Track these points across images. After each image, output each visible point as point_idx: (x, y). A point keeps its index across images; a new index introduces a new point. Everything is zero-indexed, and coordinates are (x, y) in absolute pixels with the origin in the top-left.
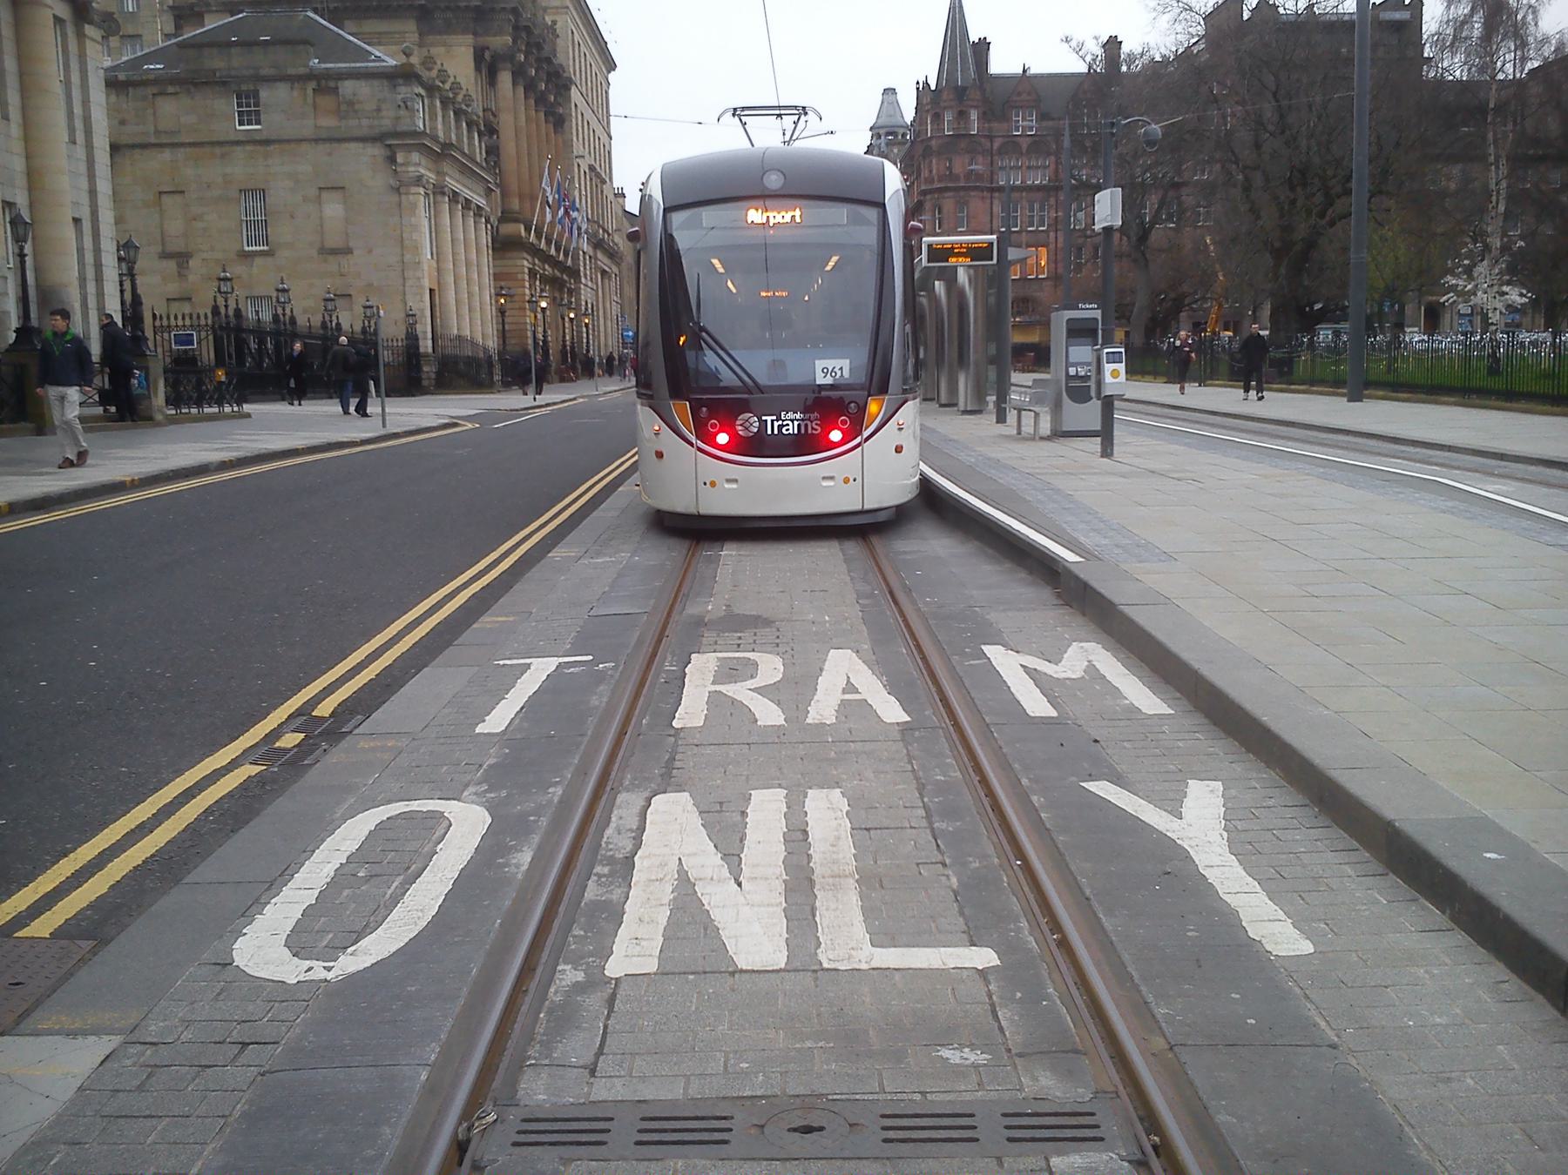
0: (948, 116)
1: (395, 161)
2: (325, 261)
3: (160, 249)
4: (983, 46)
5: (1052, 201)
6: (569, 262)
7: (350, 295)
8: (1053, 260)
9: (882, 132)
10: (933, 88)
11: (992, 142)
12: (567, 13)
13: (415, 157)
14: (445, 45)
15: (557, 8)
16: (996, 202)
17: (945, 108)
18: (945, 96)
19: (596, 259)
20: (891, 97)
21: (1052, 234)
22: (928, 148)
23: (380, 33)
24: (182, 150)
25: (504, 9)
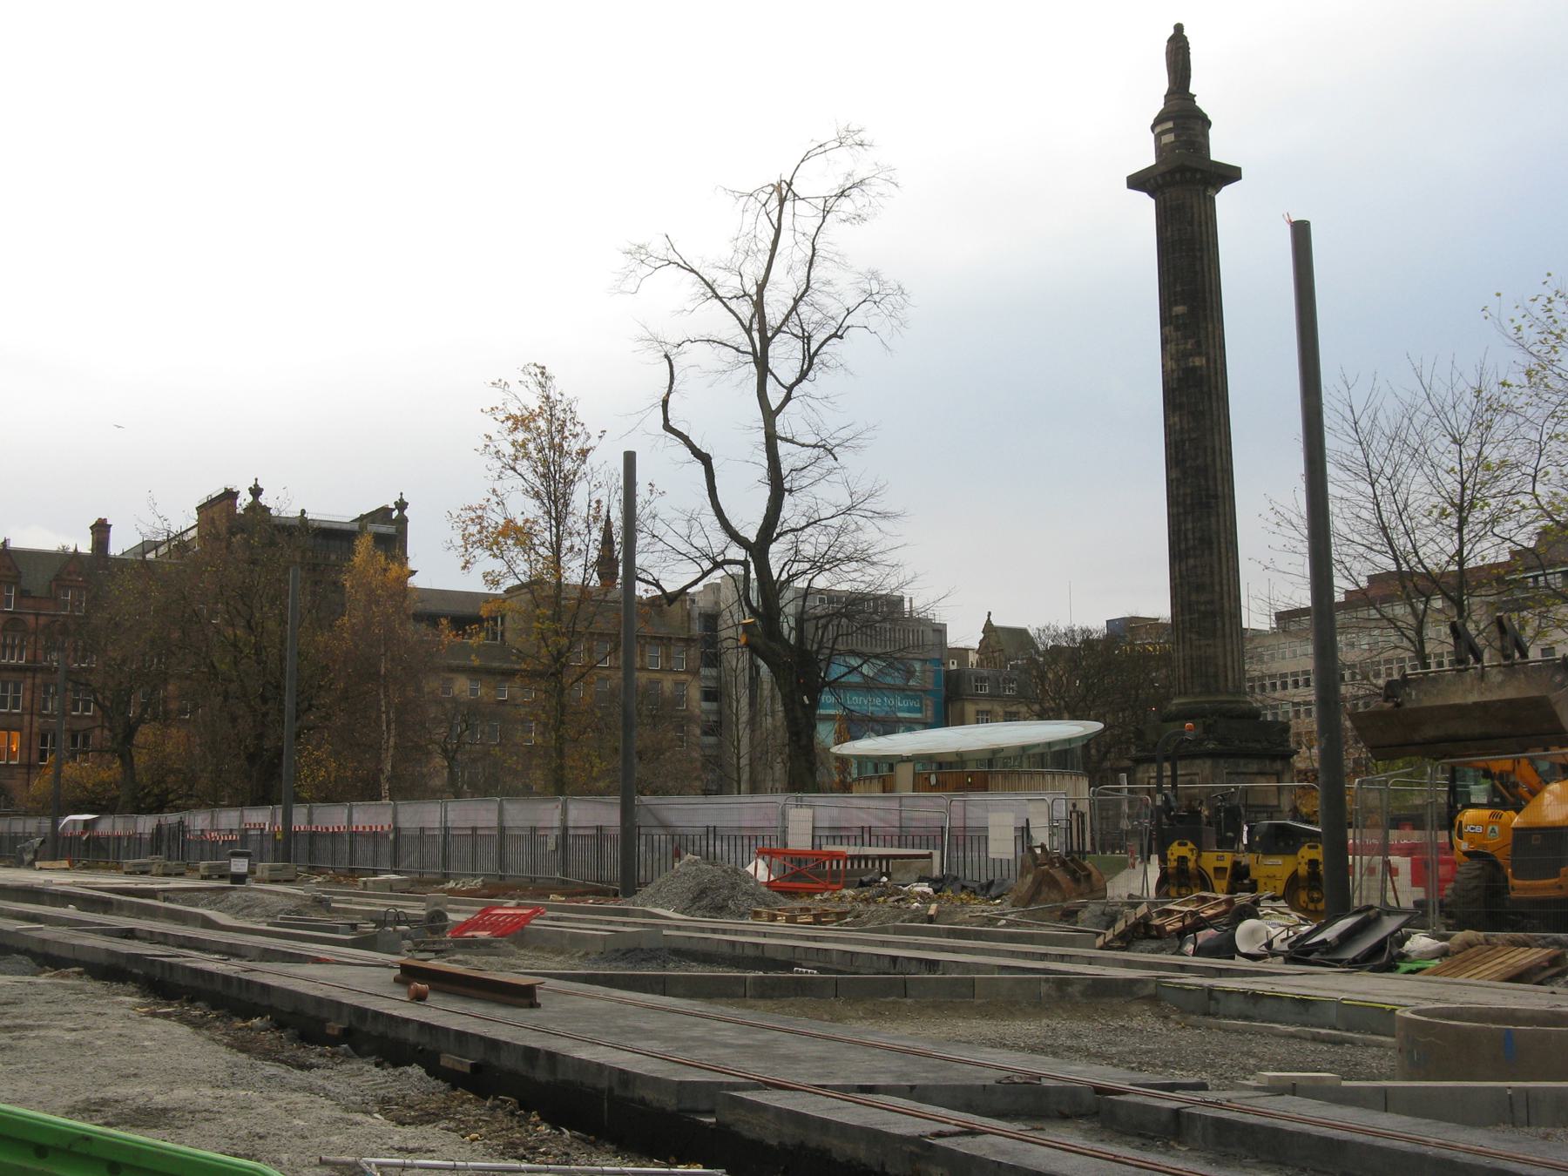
5: (29, 681)
8: (26, 746)
21: (27, 718)
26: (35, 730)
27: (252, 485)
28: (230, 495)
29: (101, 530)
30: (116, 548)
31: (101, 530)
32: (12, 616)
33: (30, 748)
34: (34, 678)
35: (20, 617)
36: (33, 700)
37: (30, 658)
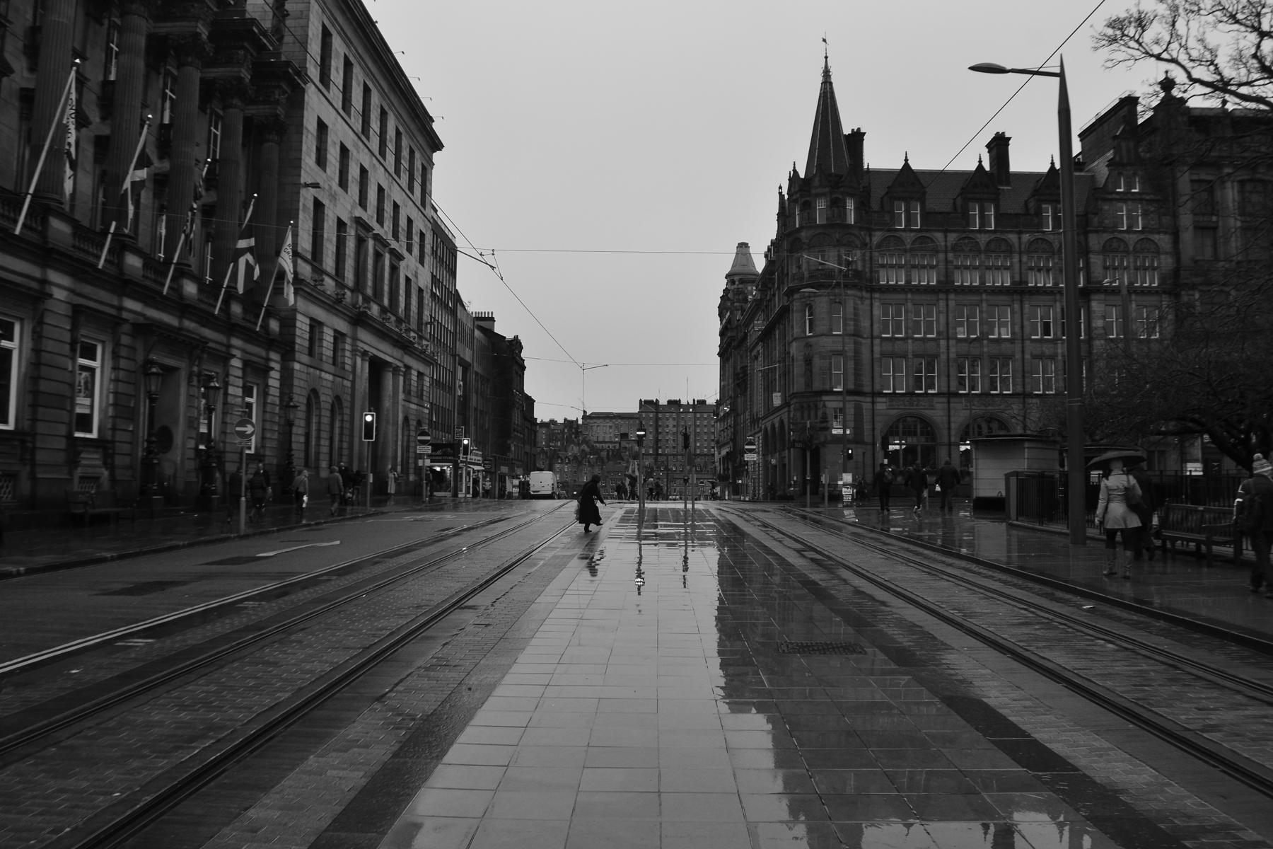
0: (821, 205)
4: (858, 137)
5: (942, 304)
6: (274, 325)
9: (736, 278)
10: (802, 175)
11: (870, 236)
16: (876, 304)
17: (818, 195)
18: (816, 182)
19: (355, 339)
20: (744, 250)
22: (799, 239)
26: (952, 356)
27: (1162, 77)
28: (1129, 103)
29: (999, 145)
30: (1017, 164)
31: (999, 145)
32: (920, 235)
33: (948, 376)
34: (947, 300)
35: (928, 235)
36: (947, 324)
37: (942, 279)
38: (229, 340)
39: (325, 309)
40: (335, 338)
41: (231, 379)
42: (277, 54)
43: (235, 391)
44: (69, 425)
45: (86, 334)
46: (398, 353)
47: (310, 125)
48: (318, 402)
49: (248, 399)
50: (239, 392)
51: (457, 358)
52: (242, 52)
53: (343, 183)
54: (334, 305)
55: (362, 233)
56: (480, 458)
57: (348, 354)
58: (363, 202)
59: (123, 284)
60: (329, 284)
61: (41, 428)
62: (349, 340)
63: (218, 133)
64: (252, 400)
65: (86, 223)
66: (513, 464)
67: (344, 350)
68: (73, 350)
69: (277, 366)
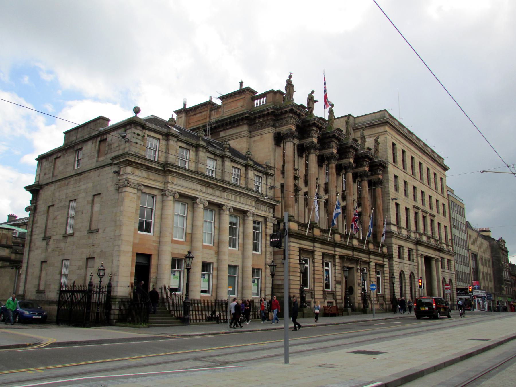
1: (120, 174)
2: (89, 238)
3: (43, 235)
6: (385, 250)
7: (94, 258)
12: (386, 134)
13: (129, 169)
14: (260, 134)
15: (382, 132)
19: (417, 250)
23: (232, 134)
24: (57, 184)
25: (286, 112)
38: (369, 256)
39: (403, 241)
40: (409, 251)
41: (371, 269)
42: (377, 157)
43: (373, 273)
44: (323, 287)
45: (326, 260)
46: (437, 253)
47: (391, 178)
48: (404, 275)
49: (378, 276)
50: (374, 273)
51: (470, 251)
52: (365, 162)
53: (406, 194)
54: (407, 239)
55: (417, 210)
56: (485, 294)
57: (415, 256)
58: (415, 199)
59: (335, 245)
60: (404, 233)
61: (316, 288)
62: (414, 251)
63: (361, 187)
64: (379, 276)
65: (324, 228)
66: (506, 296)
67: (413, 255)
68: (323, 265)
69: (387, 263)
